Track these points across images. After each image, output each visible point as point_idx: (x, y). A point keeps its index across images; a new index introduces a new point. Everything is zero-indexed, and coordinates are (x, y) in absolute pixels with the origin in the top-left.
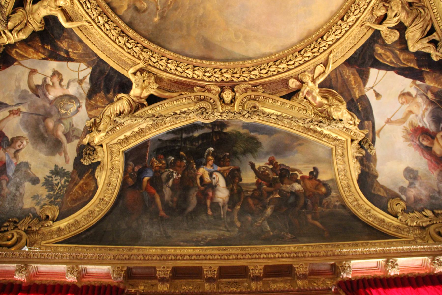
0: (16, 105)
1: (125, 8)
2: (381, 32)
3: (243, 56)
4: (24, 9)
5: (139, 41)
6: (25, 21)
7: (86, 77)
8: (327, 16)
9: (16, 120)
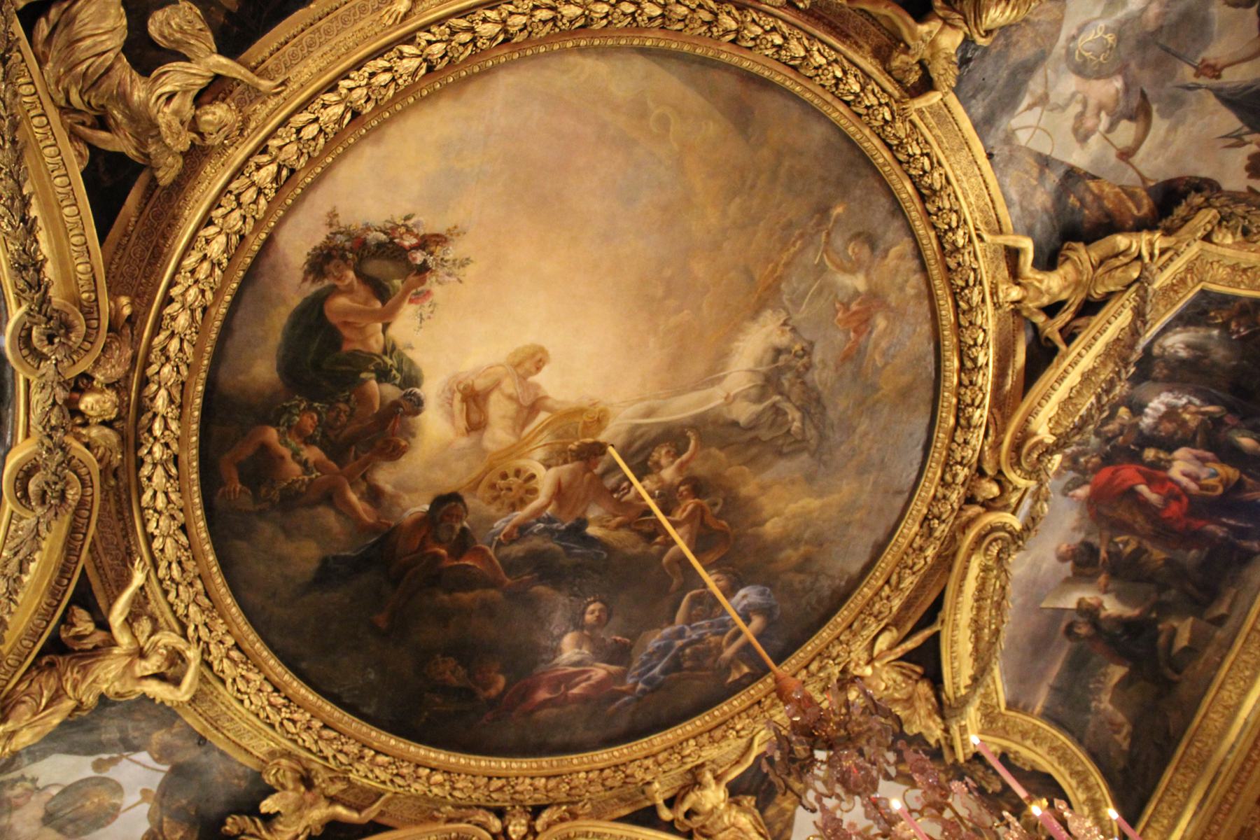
0: (1199, 87)
1: (893, 252)
2: (214, 47)
3: (662, 65)
4: (1089, 295)
5: (897, 168)
6: (1100, 271)
7: (1026, 109)
8: (393, 131)
9: (1216, 52)
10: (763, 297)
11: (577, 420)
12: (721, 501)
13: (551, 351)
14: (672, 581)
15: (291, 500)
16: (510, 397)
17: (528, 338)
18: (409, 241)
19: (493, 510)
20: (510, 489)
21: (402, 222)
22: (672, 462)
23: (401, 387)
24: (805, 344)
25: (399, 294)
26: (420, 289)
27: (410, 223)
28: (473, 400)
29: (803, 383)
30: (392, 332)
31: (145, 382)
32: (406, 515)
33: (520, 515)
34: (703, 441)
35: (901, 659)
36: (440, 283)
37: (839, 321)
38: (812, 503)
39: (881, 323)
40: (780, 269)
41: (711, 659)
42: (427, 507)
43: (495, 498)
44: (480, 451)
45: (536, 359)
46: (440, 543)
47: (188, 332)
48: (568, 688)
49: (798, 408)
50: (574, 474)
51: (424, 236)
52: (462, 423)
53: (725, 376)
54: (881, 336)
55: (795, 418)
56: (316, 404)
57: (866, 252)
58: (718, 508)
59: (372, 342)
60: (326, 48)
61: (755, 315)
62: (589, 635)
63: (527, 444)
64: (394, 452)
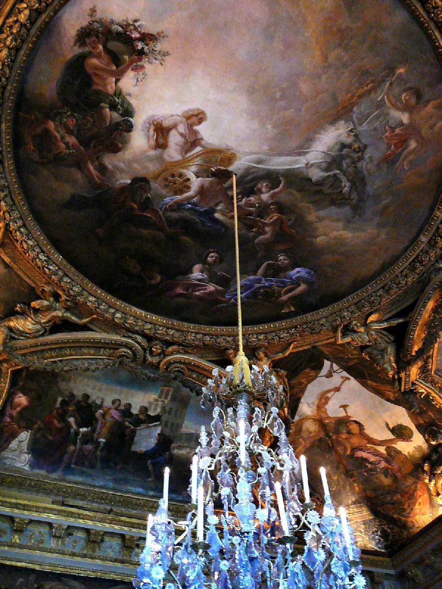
10: (341, 112)
11: (217, 155)
12: (293, 219)
13: (208, 115)
14: (258, 254)
15: (58, 160)
16: (182, 135)
17: (195, 104)
18: (135, 35)
19: (164, 192)
20: (175, 183)
21: (132, 23)
22: (269, 192)
23: (122, 115)
24: (361, 145)
25: (127, 64)
26: (139, 63)
27: (137, 24)
28: (161, 131)
29: (355, 167)
30: (120, 84)
32: (118, 183)
33: (179, 197)
34: (289, 184)
35: (384, 329)
36: (150, 62)
37: (386, 137)
38: (347, 234)
39: (413, 144)
40: (355, 98)
41: (274, 299)
42: (129, 182)
43: (166, 186)
44: (160, 158)
45: (198, 117)
46: (135, 202)
47: (6, 61)
48: (194, 291)
49: (349, 181)
50: (212, 183)
51: (144, 34)
52: (153, 142)
53: (308, 152)
54: (410, 153)
55: (346, 186)
56: (76, 114)
57: (413, 101)
58: (291, 222)
59: (109, 87)
61: (333, 121)
62: (207, 267)
63: (189, 161)
64: (115, 149)
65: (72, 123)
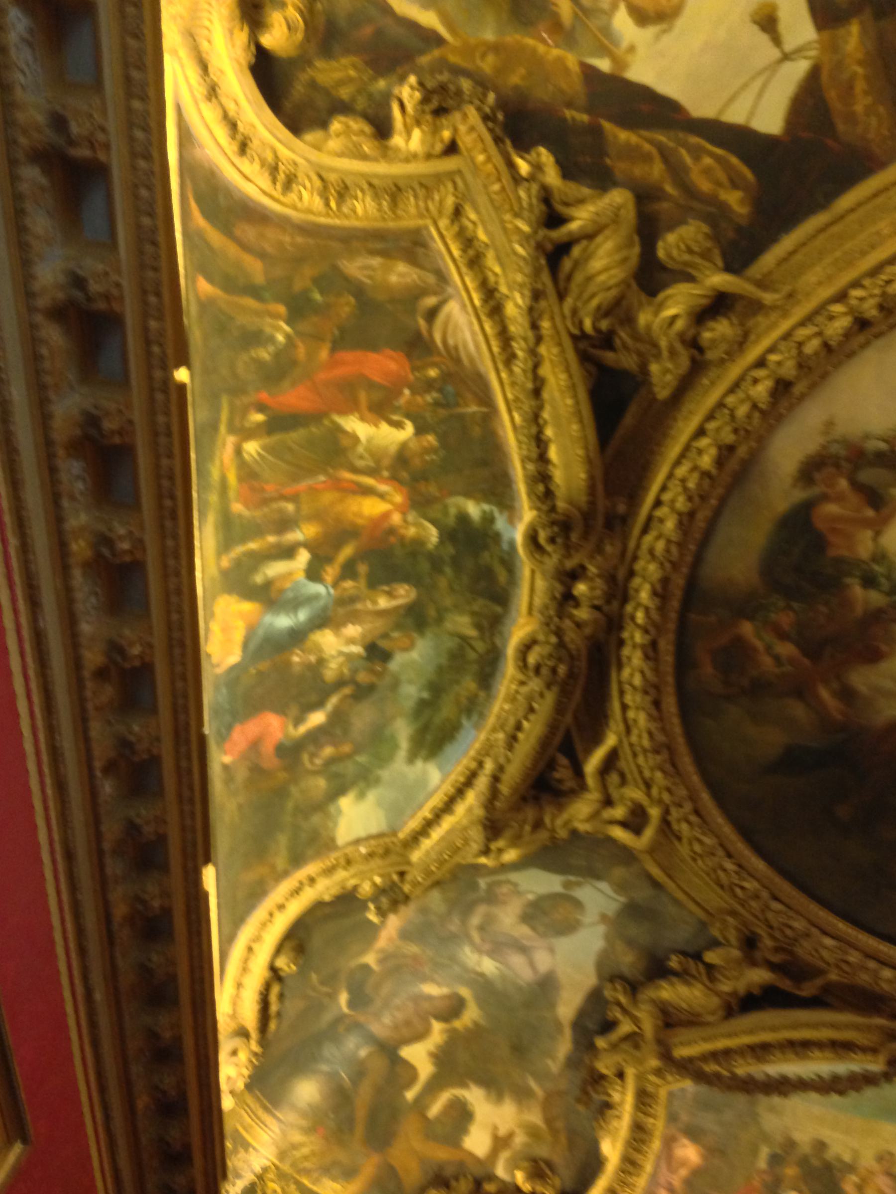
15: (759, 688)
31: (631, 574)
60: (838, 254)
65: (786, 620)
